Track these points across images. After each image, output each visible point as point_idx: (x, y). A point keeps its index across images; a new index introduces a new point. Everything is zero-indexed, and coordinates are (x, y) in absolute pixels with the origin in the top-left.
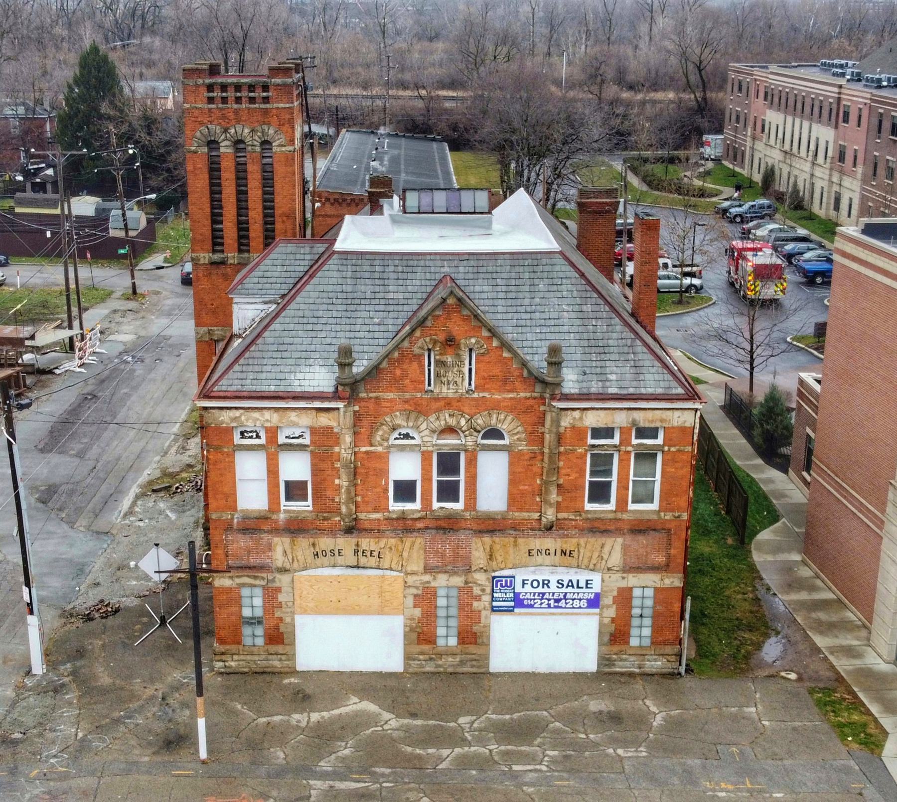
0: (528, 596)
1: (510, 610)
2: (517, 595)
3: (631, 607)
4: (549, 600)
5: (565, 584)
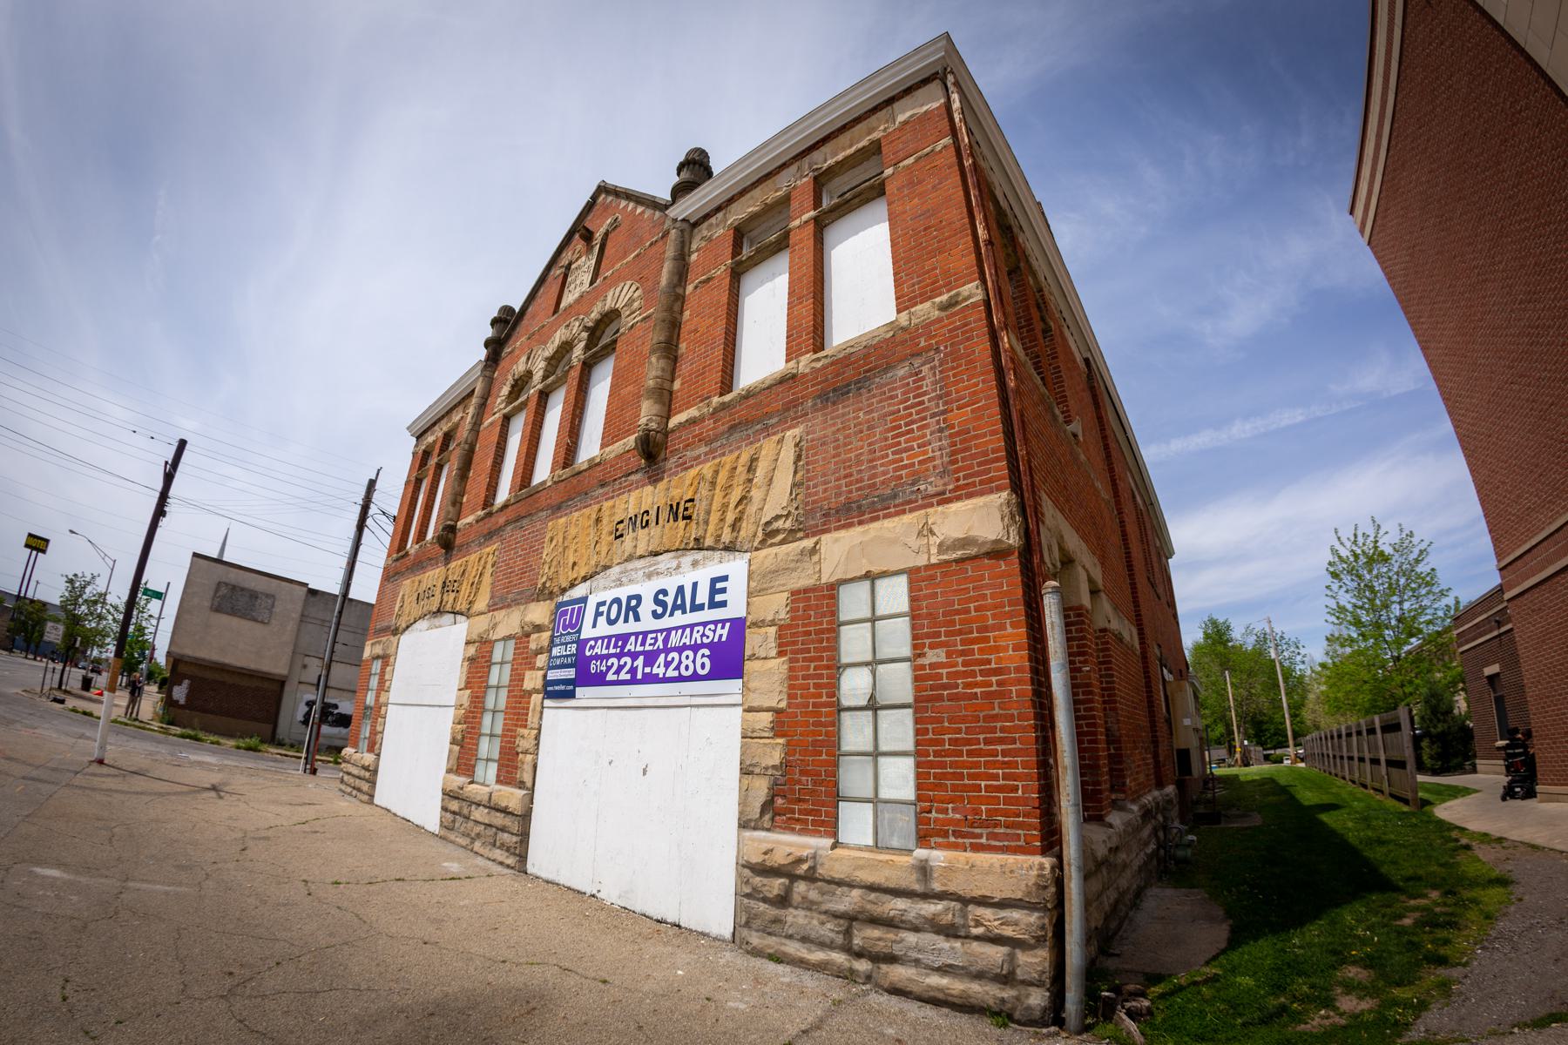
1: (561, 692)
2: (581, 644)
4: (634, 656)
5: (669, 600)
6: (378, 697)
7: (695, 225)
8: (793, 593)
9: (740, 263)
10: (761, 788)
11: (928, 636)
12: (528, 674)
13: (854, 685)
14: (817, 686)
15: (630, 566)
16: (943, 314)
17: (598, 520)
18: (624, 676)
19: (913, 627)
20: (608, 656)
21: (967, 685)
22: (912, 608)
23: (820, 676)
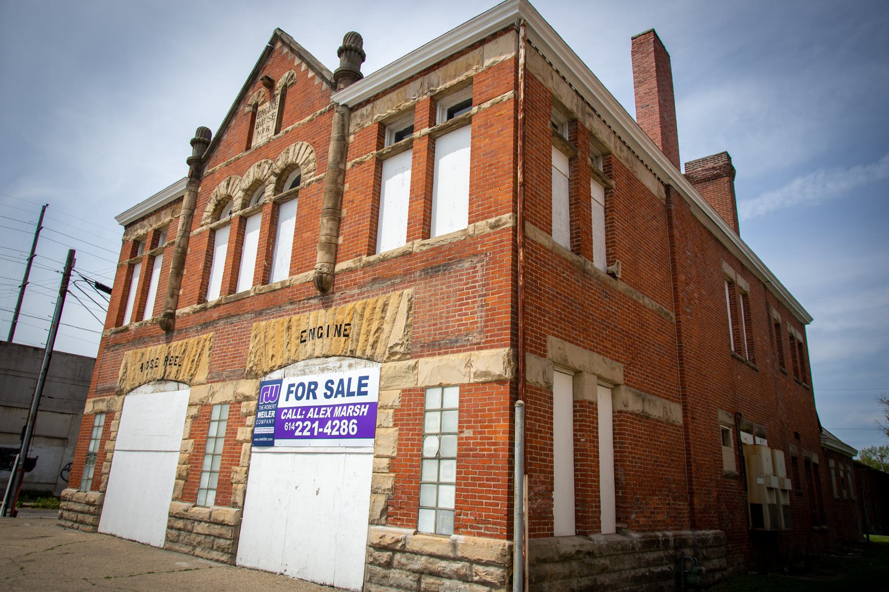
0: (289, 416)
1: (265, 442)
2: (279, 411)
3: (422, 435)
4: (313, 421)
5: (335, 387)
6: (102, 445)
7: (352, 110)
8: (404, 391)
9: (381, 155)
10: (381, 500)
11: (466, 422)
12: (240, 429)
13: (430, 446)
14: (412, 445)
15: (310, 362)
16: (491, 231)
17: (289, 328)
18: (306, 433)
19: (460, 417)
20: (296, 420)
21: (481, 450)
22: (460, 406)
23: (414, 440)
